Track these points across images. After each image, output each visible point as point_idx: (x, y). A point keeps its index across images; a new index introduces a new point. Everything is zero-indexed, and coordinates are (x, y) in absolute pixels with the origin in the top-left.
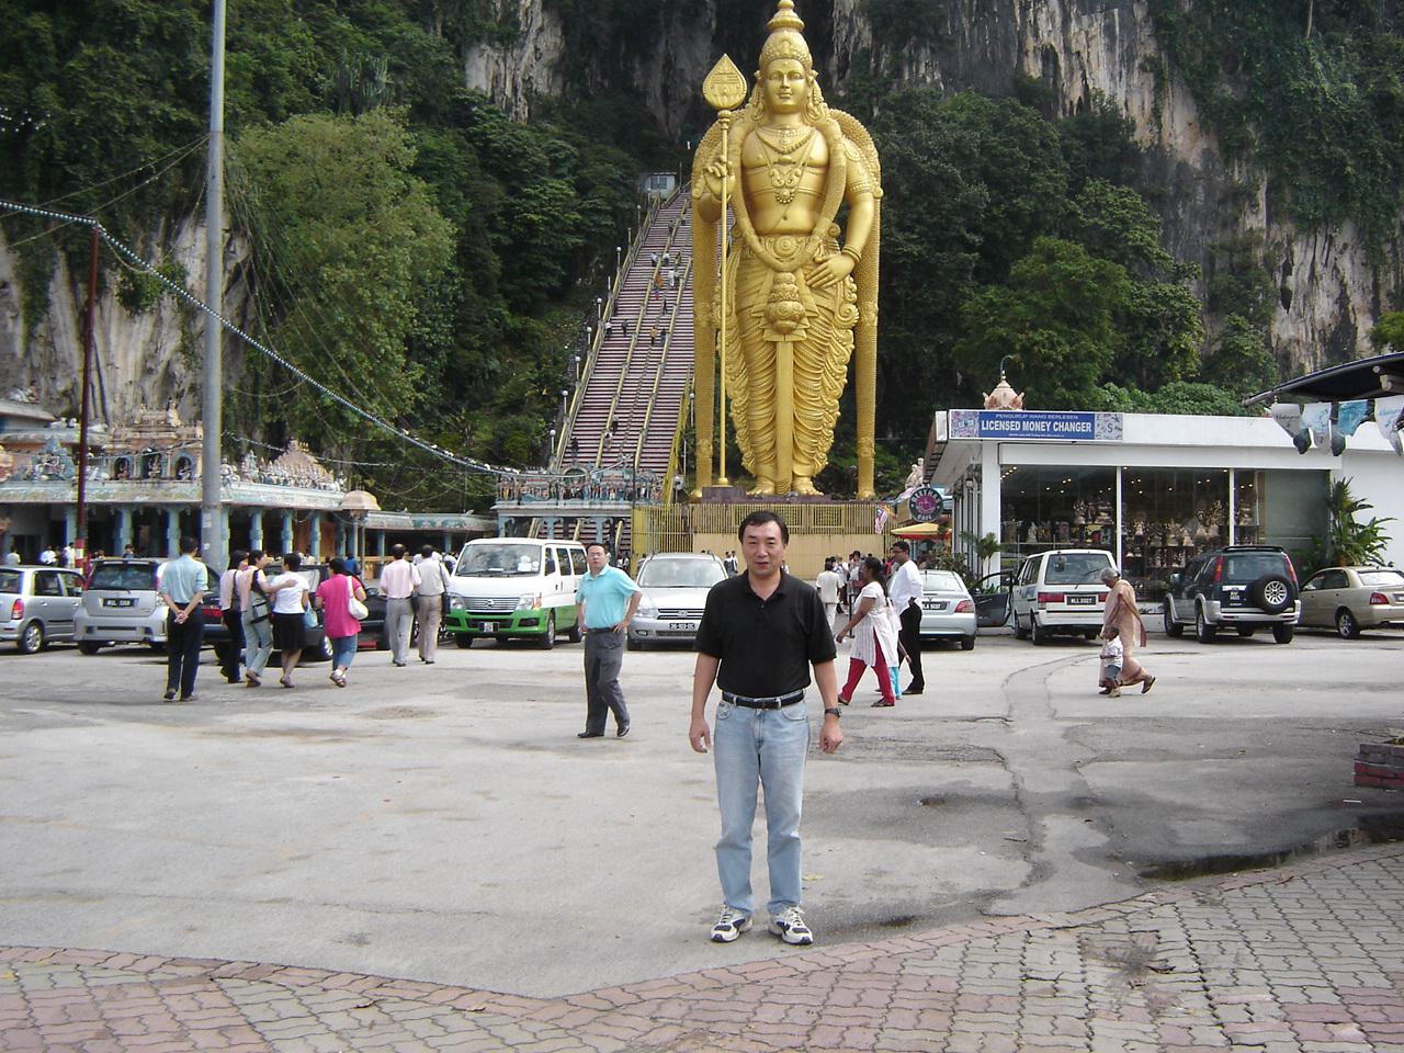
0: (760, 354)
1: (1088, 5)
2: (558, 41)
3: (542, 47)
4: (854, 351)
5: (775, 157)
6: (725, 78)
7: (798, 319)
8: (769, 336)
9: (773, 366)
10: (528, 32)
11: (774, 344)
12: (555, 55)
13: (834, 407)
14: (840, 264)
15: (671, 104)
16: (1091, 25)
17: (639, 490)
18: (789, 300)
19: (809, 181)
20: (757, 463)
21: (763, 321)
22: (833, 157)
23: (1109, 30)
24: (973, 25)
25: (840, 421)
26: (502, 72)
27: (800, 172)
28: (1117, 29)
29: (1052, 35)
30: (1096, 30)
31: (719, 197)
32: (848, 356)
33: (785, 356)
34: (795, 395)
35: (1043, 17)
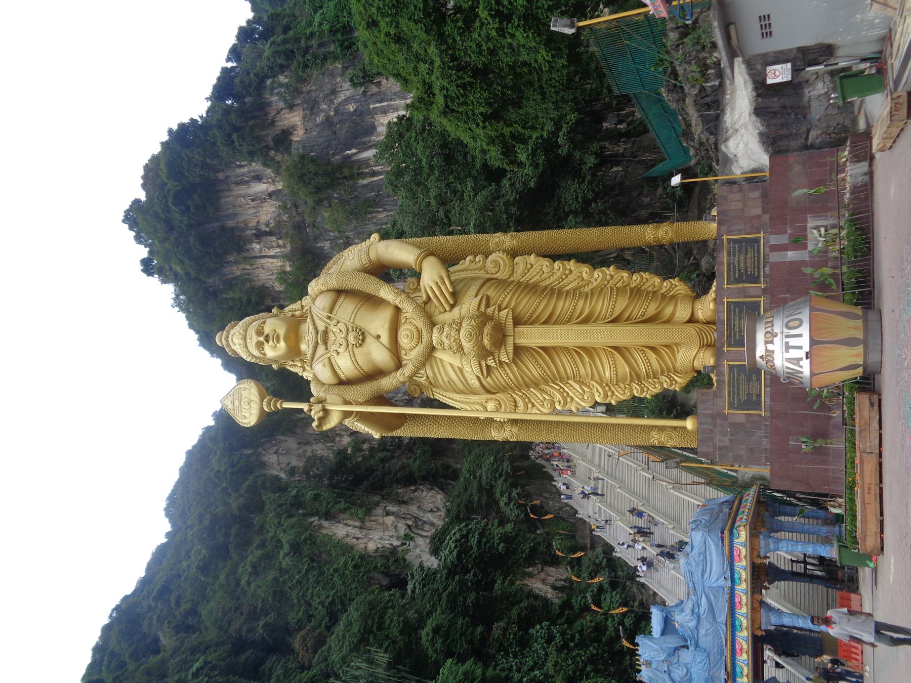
0: (532, 369)
3: (431, 506)
4: (538, 255)
5: (321, 349)
6: (237, 403)
10: (416, 518)
11: (518, 351)
14: (431, 274)
18: (459, 331)
20: (676, 371)
23: (385, 111)
24: (385, 210)
25: (618, 268)
27: (334, 322)
33: (531, 337)
34: (586, 321)
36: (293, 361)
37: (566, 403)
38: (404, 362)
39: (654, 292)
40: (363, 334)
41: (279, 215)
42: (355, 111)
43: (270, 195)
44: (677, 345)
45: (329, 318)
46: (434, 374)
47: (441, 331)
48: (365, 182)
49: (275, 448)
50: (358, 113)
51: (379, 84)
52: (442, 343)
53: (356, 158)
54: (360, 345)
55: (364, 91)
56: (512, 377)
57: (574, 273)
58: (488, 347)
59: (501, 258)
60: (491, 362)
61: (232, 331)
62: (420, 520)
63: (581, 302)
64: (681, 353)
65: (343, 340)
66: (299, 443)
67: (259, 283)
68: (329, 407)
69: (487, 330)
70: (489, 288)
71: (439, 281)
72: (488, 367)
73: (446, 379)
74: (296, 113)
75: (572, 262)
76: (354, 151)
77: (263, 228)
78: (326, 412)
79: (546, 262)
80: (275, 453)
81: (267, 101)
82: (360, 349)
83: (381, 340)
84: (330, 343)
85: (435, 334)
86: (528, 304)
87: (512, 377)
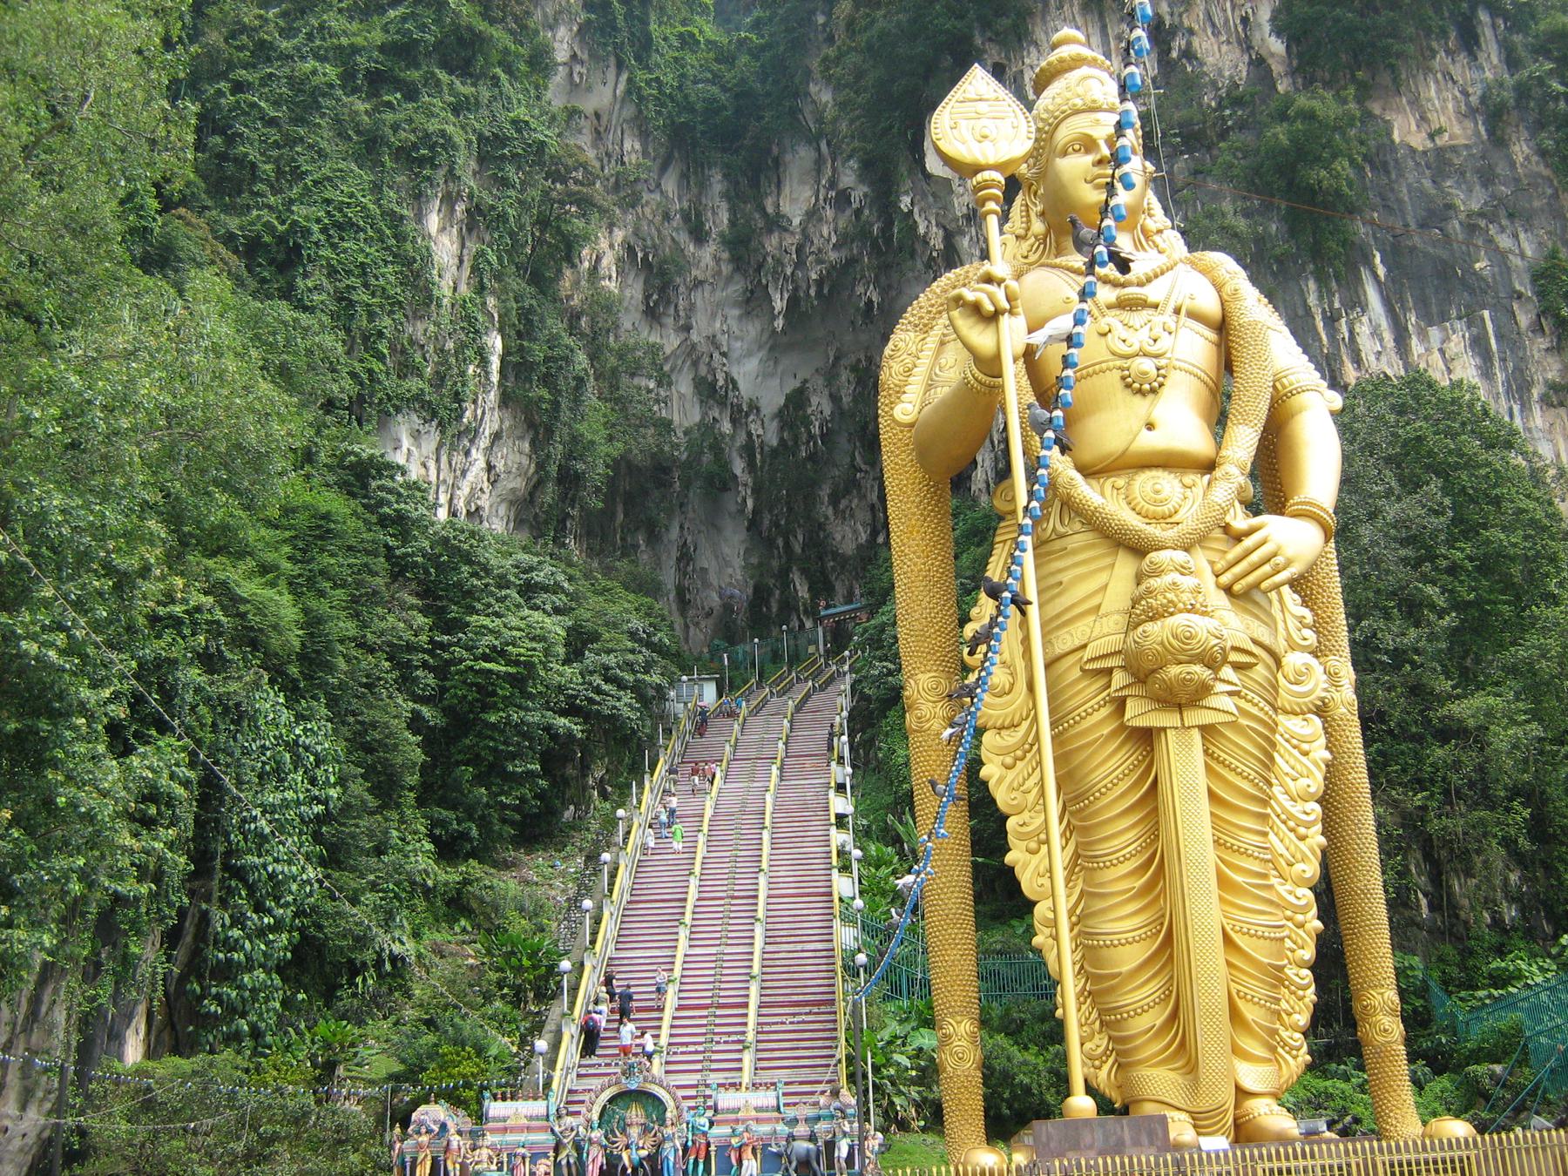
1: (1434, 309)
2: (525, 461)
3: (500, 466)
7: (1212, 662)
8: (1138, 713)
9: (1151, 799)
12: (518, 483)
13: (1304, 910)
15: (691, 613)
16: (1446, 339)
17: (831, 1146)
18: (1192, 610)
19: (1194, 348)
21: (1119, 679)
22: (1232, 307)
23: (1478, 344)
26: (433, 478)
28: (1493, 341)
29: (1384, 358)
30: (1458, 343)
31: (990, 365)
32: (1319, 777)
33: (1184, 762)
35: (1363, 330)
36: (1042, 214)
37: (1022, 837)
38: (1094, 482)
39: (1277, 1014)
40: (1153, 391)
41: (1214, 83)
42: (1475, 273)
43: (1259, 63)
44: (1191, 1069)
45: (1177, 311)
46: (1074, 552)
47: (1184, 570)
48: (1312, 300)
49: (585, 57)
50: (1472, 280)
51: (1538, 328)
52: (1157, 572)
53: (1365, 274)
54: (1128, 386)
55: (1520, 296)
56: (1086, 724)
57: (1301, 844)
58: (1161, 675)
59: (1316, 685)
60: (1119, 679)
61: (1105, 76)
62: (472, 441)
63: (1256, 867)
64: (1172, 1075)
65: (1136, 348)
66: (597, 115)
67: (1039, 34)
68: (1005, 320)
69: (1200, 671)
70: (1268, 667)
71: (1279, 560)
72: (1109, 672)
73: (1066, 577)
74: (1457, 130)
75: (1323, 840)
76: (1381, 271)
77: (1178, 43)
78: (993, 318)
79: (1316, 783)
80: (574, 57)
81: (1482, 56)
82: (1119, 385)
83: (1144, 430)
84: (1126, 316)
85: (1180, 556)
86: (1240, 750)
87: (1086, 724)
